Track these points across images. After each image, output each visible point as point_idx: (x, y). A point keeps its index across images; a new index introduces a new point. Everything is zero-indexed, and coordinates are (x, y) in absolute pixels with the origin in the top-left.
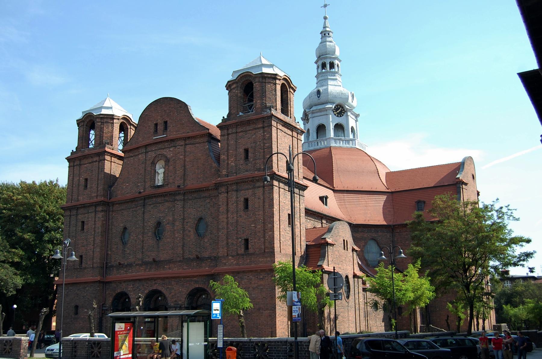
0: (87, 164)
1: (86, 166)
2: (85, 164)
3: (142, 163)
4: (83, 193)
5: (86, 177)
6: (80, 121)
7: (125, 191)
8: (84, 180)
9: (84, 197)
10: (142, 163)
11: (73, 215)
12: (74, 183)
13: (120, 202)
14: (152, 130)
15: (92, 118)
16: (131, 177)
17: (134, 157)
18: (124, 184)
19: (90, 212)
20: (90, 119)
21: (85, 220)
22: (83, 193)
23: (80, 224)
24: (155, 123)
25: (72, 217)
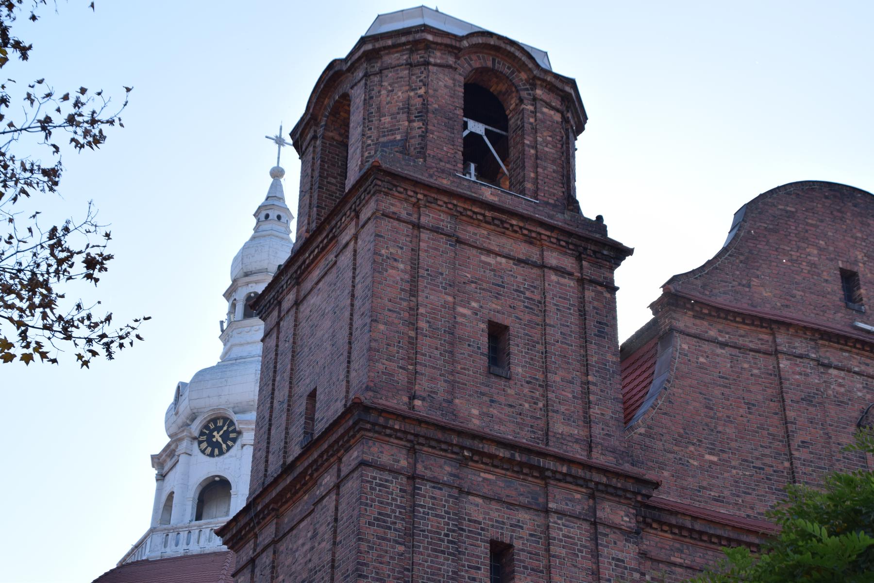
0: (504, 260)
1: (490, 260)
2: (489, 252)
3: (808, 400)
4: (484, 389)
5: (500, 319)
6: (447, 41)
7: (705, 484)
8: (484, 326)
9: (494, 411)
10: (808, 400)
11: (436, 483)
12: (422, 310)
13: (698, 526)
14: (835, 288)
15: (504, 68)
16: (730, 431)
17: (735, 352)
18: (692, 448)
19: (561, 514)
20: (489, 64)
21: (518, 544)
22: (484, 389)
23: (483, 550)
24: (841, 266)
25: (426, 489)
